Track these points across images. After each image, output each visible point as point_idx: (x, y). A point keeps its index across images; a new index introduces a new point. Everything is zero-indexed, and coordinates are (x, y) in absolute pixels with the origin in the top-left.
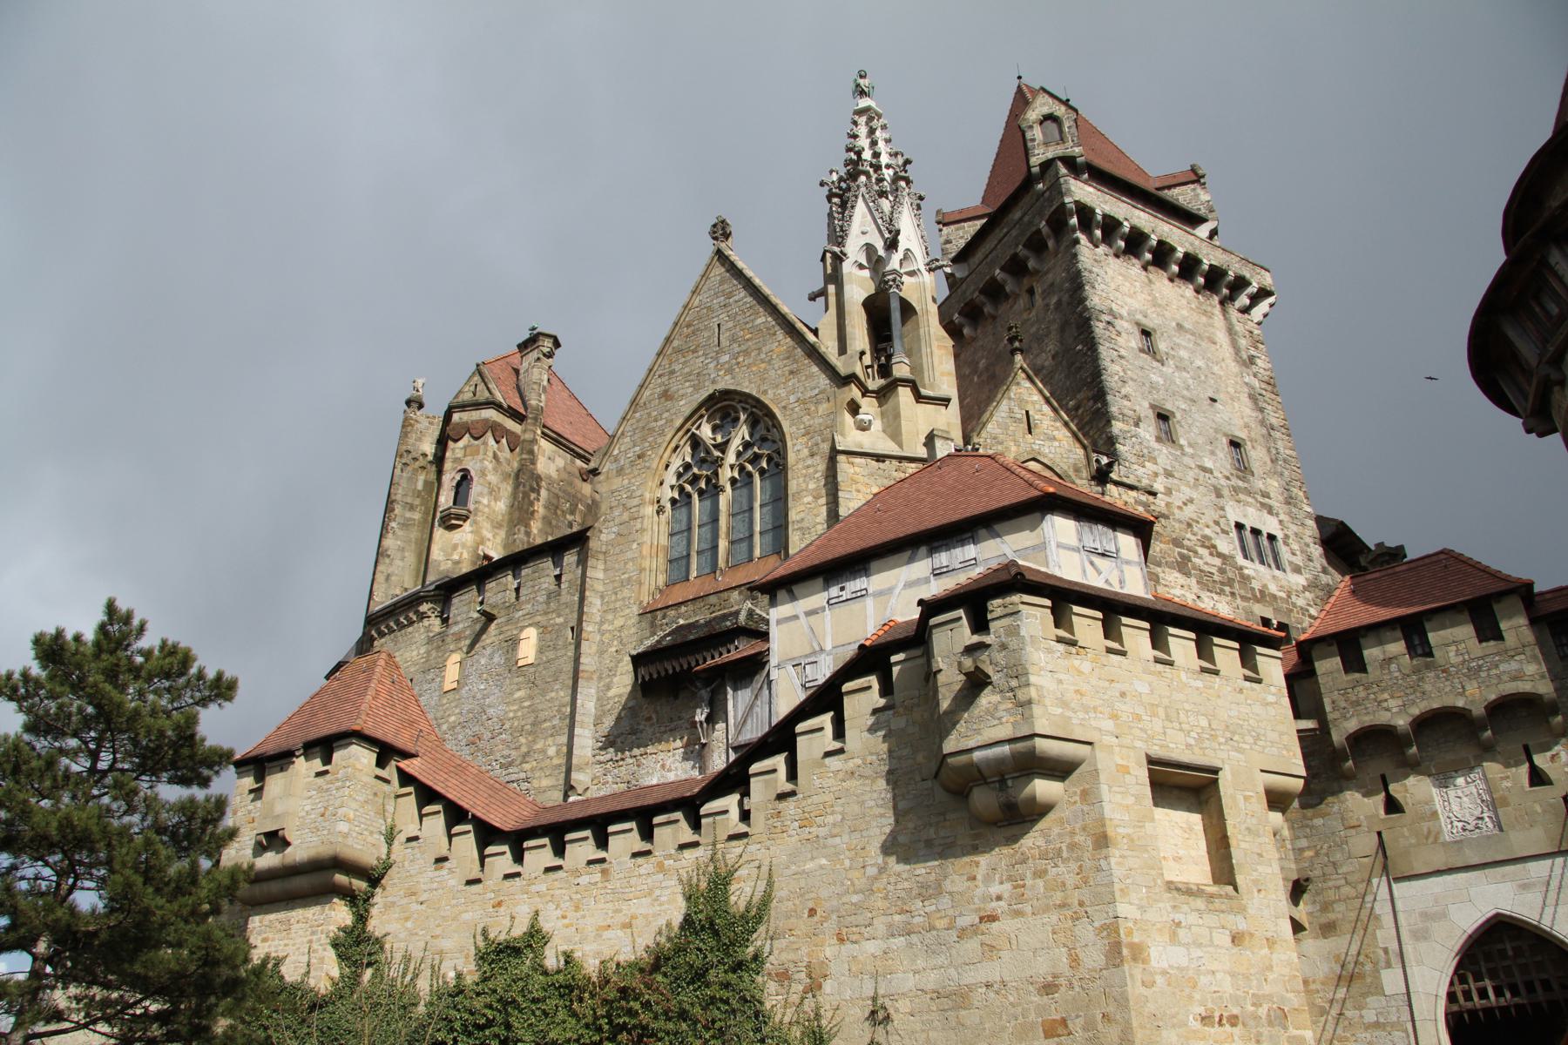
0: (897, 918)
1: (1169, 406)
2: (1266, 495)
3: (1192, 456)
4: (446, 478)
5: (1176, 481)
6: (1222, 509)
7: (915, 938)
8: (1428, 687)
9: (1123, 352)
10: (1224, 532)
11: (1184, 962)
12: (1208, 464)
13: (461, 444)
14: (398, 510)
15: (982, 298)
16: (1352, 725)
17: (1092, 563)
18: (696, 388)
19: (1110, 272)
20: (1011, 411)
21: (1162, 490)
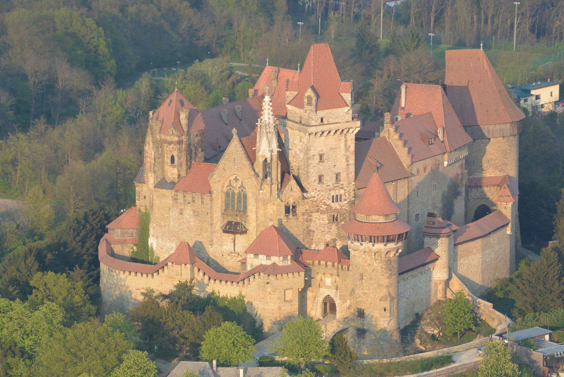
2: (342, 185)
3: (326, 184)
9: (315, 165)
10: (329, 199)
12: (329, 184)
13: (171, 146)
14: (156, 159)
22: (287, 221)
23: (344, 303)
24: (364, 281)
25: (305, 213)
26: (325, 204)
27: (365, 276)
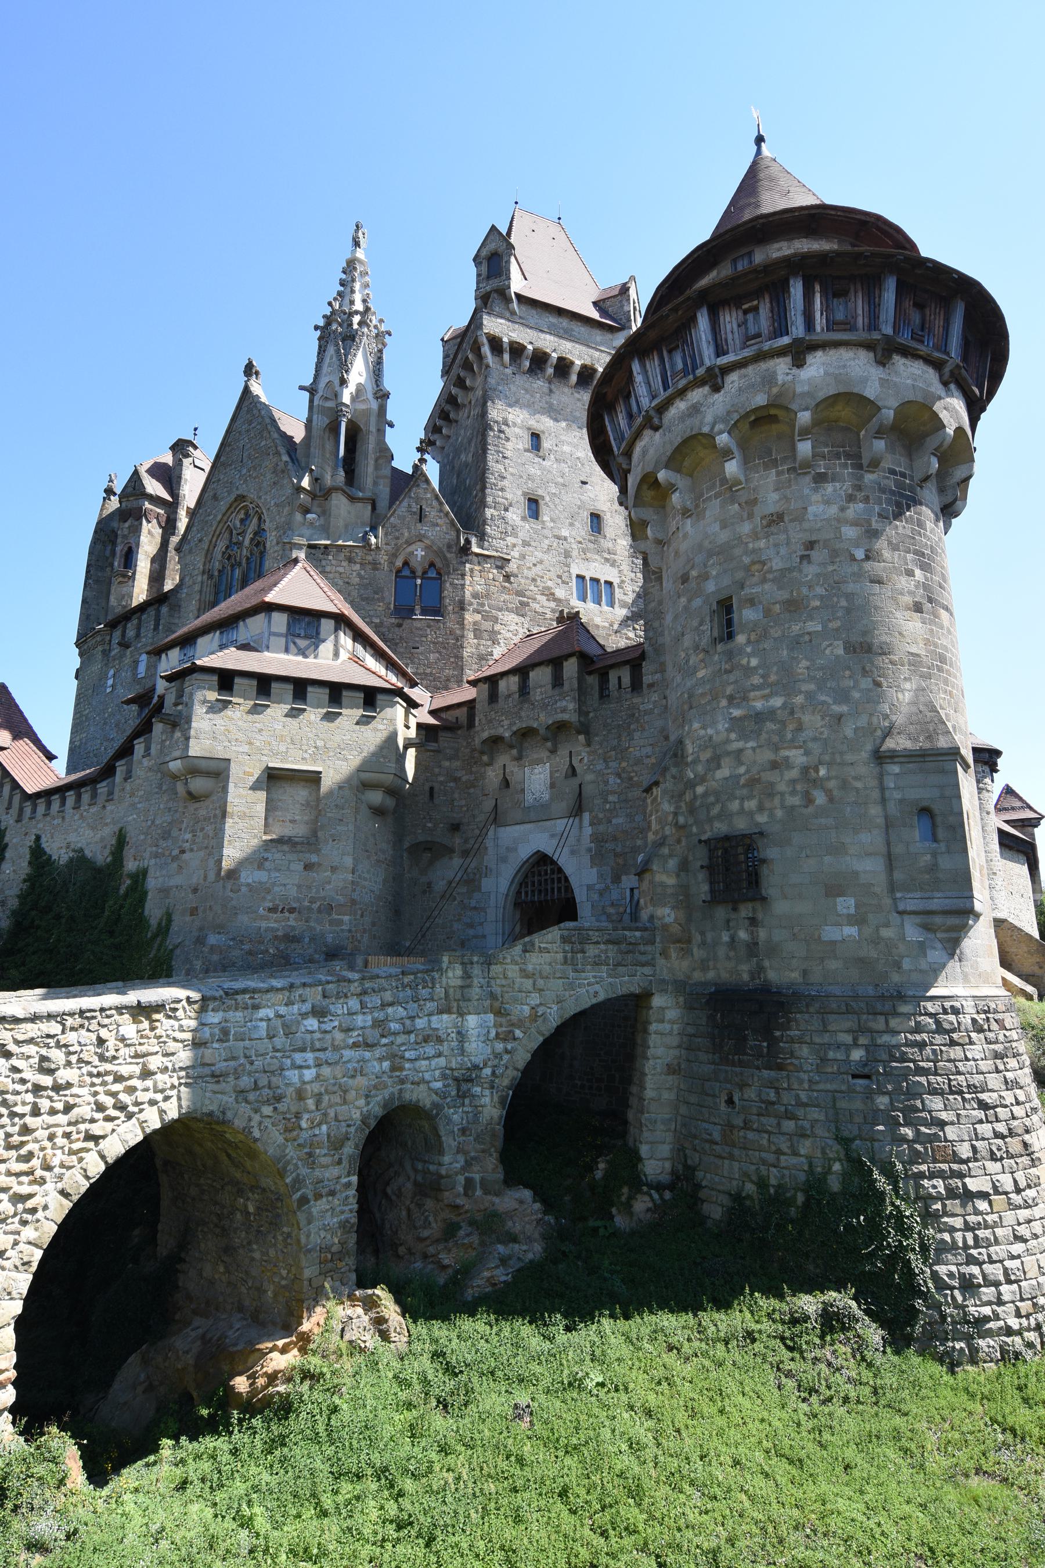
0: (154, 849)
1: (540, 492)
4: (118, 549)
5: (531, 549)
6: (568, 566)
7: (158, 860)
8: (523, 714)
9: (508, 454)
10: (564, 582)
11: (264, 879)
12: (565, 533)
13: (127, 525)
15: (448, 407)
16: (485, 735)
17: (295, 643)
18: (229, 493)
19: (513, 388)
20: (409, 506)
21: (517, 555)
22: (400, 625)
23: (617, 879)
24: (741, 639)
25: (471, 604)
26: (551, 596)
27: (751, 602)
